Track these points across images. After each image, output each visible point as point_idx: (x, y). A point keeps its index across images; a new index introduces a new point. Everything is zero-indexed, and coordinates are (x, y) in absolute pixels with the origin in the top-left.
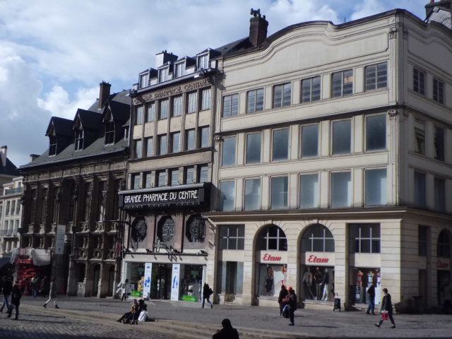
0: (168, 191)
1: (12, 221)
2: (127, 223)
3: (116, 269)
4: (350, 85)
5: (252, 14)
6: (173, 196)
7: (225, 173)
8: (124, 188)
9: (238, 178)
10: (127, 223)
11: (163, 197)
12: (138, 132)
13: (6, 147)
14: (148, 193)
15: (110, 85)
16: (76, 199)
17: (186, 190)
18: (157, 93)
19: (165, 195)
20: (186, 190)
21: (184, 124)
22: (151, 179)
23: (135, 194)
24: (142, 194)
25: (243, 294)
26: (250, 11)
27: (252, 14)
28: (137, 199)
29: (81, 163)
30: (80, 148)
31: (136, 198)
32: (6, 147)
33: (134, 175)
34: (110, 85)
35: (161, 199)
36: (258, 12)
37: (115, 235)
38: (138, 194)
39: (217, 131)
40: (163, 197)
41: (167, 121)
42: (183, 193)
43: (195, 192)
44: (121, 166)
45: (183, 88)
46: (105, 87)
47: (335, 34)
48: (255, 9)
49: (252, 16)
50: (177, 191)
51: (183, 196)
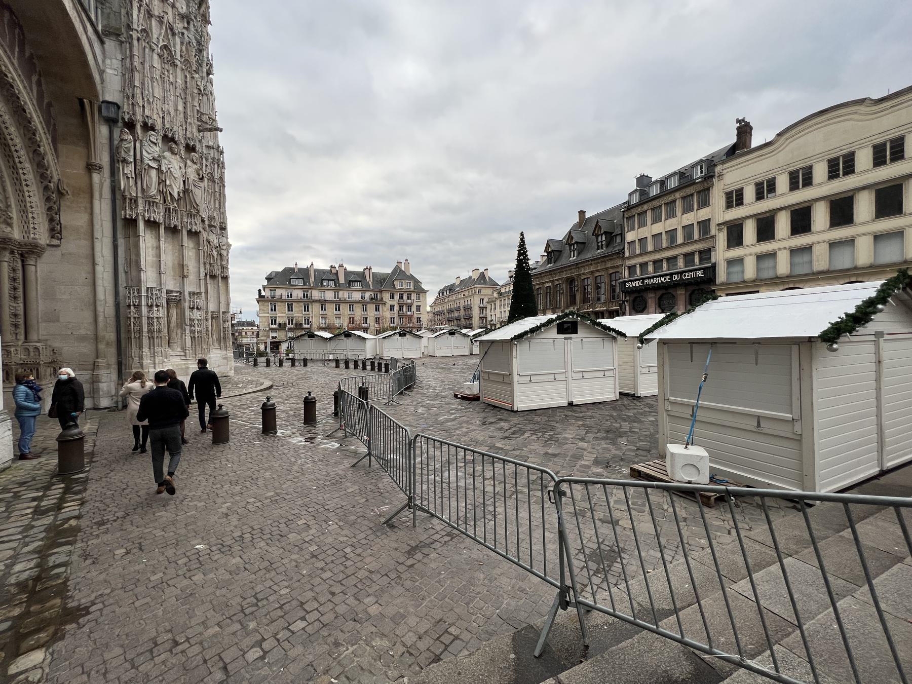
0: (671, 275)
2: (627, 301)
6: (676, 278)
9: (748, 255)
10: (627, 301)
11: (665, 279)
12: (630, 236)
14: (649, 278)
15: (585, 212)
16: (578, 290)
17: (691, 271)
18: (650, 204)
19: (668, 278)
20: (691, 271)
21: (680, 222)
22: (650, 268)
23: (636, 280)
24: (643, 279)
28: (638, 284)
29: (577, 265)
30: (574, 256)
31: (637, 283)
33: (629, 268)
34: (585, 212)
35: (663, 281)
36: (743, 120)
38: (639, 280)
40: (665, 279)
42: (687, 274)
43: (702, 271)
44: (619, 263)
45: (678, 195)
46: (582, 213)
47: (874, 108)
48: (740, 118)
49: (738, 125)
50: (681, 273)
51: (687, 276)
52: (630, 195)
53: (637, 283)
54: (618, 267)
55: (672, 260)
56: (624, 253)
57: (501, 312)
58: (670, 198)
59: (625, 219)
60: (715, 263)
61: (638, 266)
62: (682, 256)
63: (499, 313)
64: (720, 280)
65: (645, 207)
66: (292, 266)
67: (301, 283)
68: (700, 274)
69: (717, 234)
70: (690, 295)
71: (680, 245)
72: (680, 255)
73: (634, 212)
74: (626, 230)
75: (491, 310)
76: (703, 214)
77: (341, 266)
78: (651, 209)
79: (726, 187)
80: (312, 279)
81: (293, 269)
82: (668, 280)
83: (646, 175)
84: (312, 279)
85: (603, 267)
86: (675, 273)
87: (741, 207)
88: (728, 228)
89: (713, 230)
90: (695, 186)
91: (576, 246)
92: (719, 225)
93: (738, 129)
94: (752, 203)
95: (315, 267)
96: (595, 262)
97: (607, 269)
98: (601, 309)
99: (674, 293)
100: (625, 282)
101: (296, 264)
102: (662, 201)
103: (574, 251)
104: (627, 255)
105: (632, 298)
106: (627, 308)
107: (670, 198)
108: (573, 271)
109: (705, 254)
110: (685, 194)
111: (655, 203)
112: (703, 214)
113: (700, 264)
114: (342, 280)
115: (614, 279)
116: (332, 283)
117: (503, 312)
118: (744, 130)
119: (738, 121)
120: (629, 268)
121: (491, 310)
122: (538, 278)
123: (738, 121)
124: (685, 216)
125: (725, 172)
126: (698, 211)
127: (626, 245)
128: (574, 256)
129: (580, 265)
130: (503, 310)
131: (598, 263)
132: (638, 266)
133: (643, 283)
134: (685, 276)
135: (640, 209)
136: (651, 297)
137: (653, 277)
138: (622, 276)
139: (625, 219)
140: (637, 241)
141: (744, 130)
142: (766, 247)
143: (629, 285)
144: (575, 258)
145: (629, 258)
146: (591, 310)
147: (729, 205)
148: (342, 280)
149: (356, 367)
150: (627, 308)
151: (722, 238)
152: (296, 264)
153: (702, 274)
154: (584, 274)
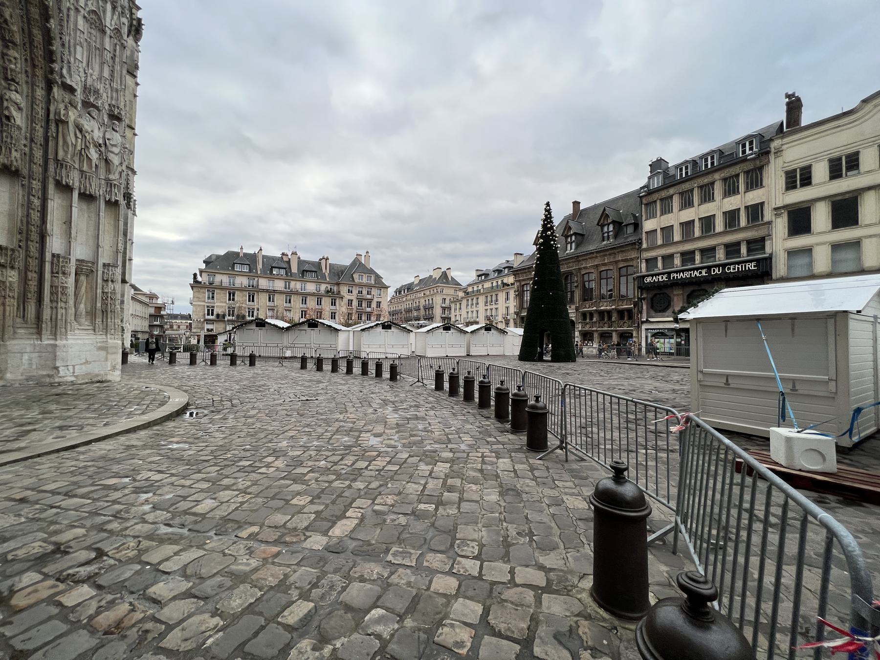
10: (644, 299)
11: (700, 273)
12: (648, 225)
14: (676, 272)
18: (677, 187)
22: (677, 261)
24: (669, 273)
26: (784, 96)
30: (571, 249)
33: (647, 261)
35: (698, 275)
36: (793, 95)
40: (700, 273)
42: (732, 267)
43: (753, 264)
44: (633, 255)
45: (717, 176)
46: (576, 204)
48: (790, 93)
49: (787, 100)
50: (724, 266)
53: (660, 277)
54: (632, 259)
55: (708, 252)
56: (641, 243)
57: (468, 312)
59: (643, 206)
60: (771, 255)
61: (660, 259)
62: (723, 246)
63: (466, 313)
64: (778, 274)
65: (671, 191)
66: (237, 250)
67: (246, 269)
68: (752, 266)
69: (774, 220)
71: (720, 233)
72: (719, 245)
73: (655, 196)
74: (644, 218)
75: (456, 309)
76: (754, 197)
77: (294, 253)
79: (786, 165)
80: (260, 266)
81: (237, 254)
82: (704, 274)
84: (260, 266)
85: (612, 260)
86: (716, 266)
88: (789, 213)
89: (768, 215)
90: (747, 163)
92: (776, 209)
93: (788, 104)
94: (824, 183)
95: (264, 253)
96: (601, 254)
97: (617, 262)
98: (608, 308)
100: (644, 277)
101: (242, 248)
102: (695, 184)
103: (571, 243)
104: (644, 246)
105: (650, 296)
106: (645, 307)
107: (706, 181)
108: (571, 265)
109: (757, 244)
110: (728, 175)
112: (754, 197)
113: (748, 255)
114: (294, 269)
115: (625, 274)
116: (283, 272)
117: (470, 313)
118: (794, 106)
119: (788, 96)
120: (647, 261)
121: (456, 309)
122: (525, 273)
123: (788, 96)
124: (726, 200)
125: (784, 147)
126: (747, 194)
127: (644, 235)
129: (580, 259)
130: (470, 310)
131: (606, 255)
132: (660, 259)
133: (669, 277)
134: (729, 269)
135: (664, 194)
137: (683, 271)
139: (643, 206)
140: (659, 231)
141: (794, 106)
143: (649, 280)
144: (572, 251)
145: (647, 250)
146: (595, 308)
147: (791, 185)
148: (294, 269)
149: (335, 369)
150: (645, 307)
151: (781, 225)
152: (242, 248)
153: (754, 266)
154: (585, 268)
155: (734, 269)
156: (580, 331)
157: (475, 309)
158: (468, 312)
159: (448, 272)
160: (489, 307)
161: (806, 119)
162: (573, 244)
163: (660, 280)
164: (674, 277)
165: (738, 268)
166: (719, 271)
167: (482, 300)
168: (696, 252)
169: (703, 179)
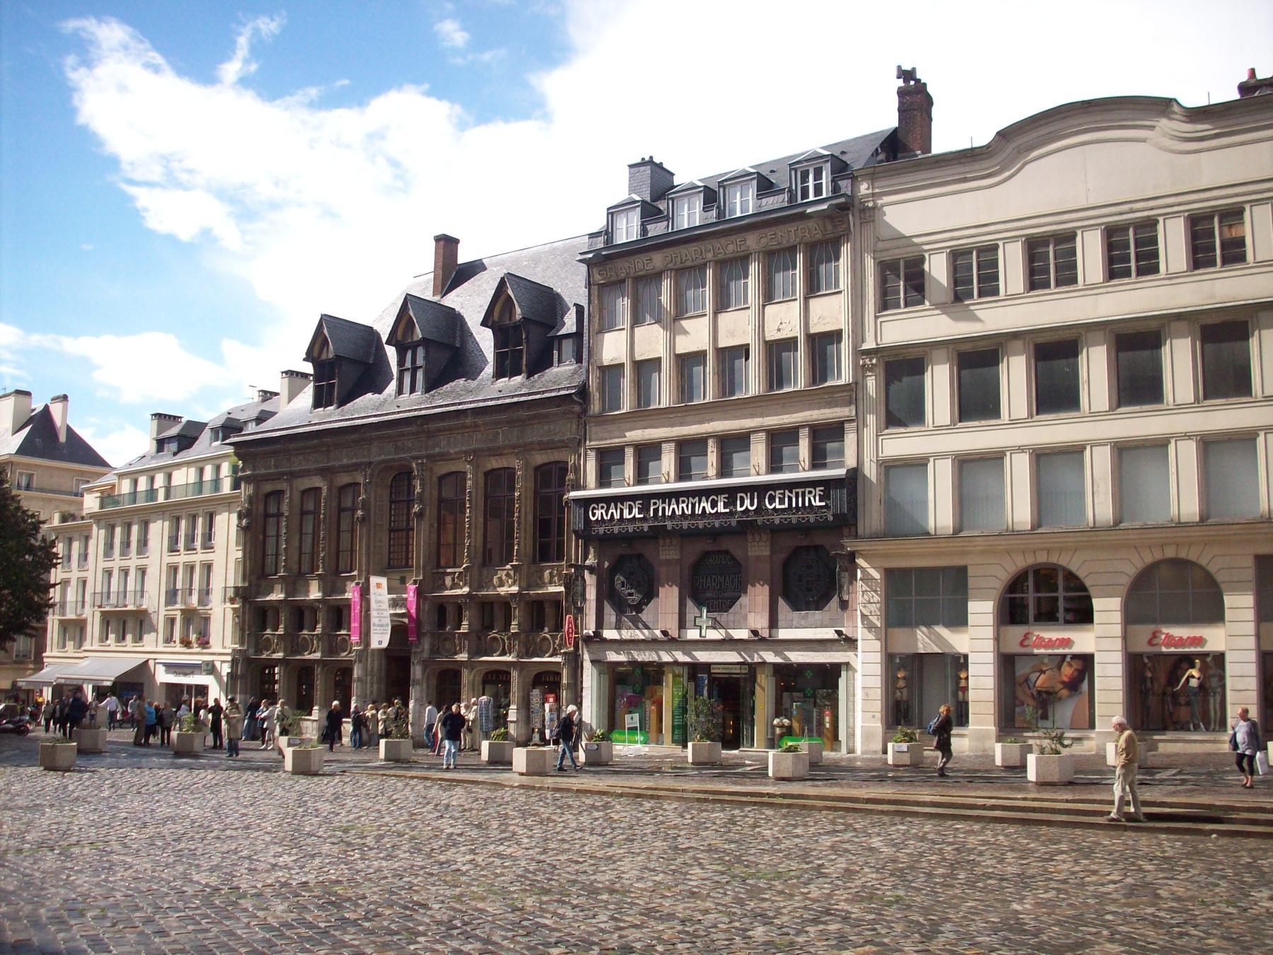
1: (191, 568)
2: (591, 569)
3: (565, 681)
4: (1241, 242)
5: (899, 77)
7: (900, 444)
8: (577, 487)
13: (65, 398)
15: (456, 241)
16: (420, 515)
24: (646, 498)
25: (971, 727)
26: (895, 73)
27: (899, 77)
30: (413, 390)
32: (65, 398)
34: (456, 241)
35: (709, 509)
37: (555, 600)
39: (869, 344)
40: (714, 504)
41: (705, 322)
42: (778, 494)
44: (568, 430)
45: (752, 241)
50: (760, 490)
52: (613, 212)
55: (733, 444)
57: (109, 573)
58: (730, 247)
61: (629, 452)
62: (763, 436)
70: (786, 565)
72: (756, 431)
78: (677, 270)
79: (880, 245)
82: (721, 508)
83: (657, 160)
87: (1236, 270)
90: (802, 225)
91: (421, 352)
93: (901, 93)
96: (488, 419)
99: (738, 553)
102: (709, 251)
107: (731, 248)
110: (773, 245)
111: (689, 253)
120: (602, 454)
122: (274, 453)
128: (413, 390)
132: (629, 452)
134: (772, 500)
135: (641, 264)
136: (669, 562)
138: (578, 479)
142: (977, 437)
154: (444, 457)
155: (782, 502)
156: (425, 664)
157: (133, 562)
158: (109, 573)
159: (56, 410)
160: (182, 558)
161: (945, 138)
162: (420, 375)
163: (626, 515)
164: (656, 511)
165: (790, 499)
166: (752, 504)
167: (159, 530)
168: (711, 442)
169: (723, 241)
